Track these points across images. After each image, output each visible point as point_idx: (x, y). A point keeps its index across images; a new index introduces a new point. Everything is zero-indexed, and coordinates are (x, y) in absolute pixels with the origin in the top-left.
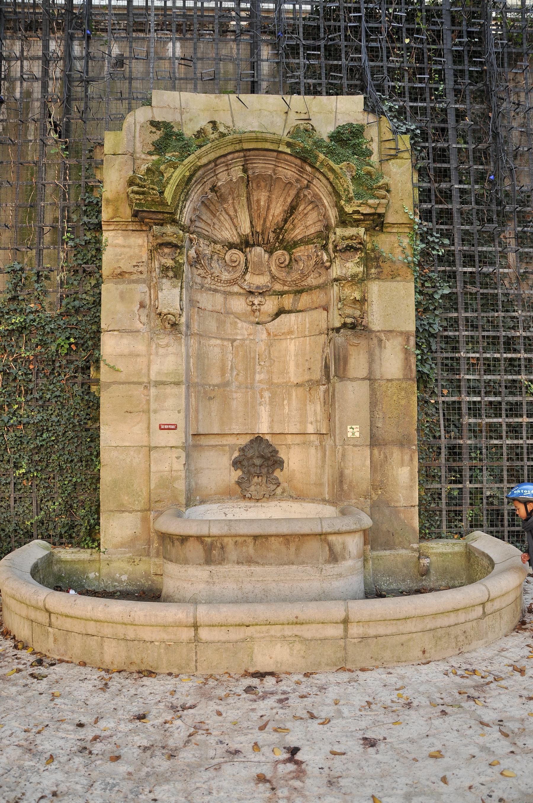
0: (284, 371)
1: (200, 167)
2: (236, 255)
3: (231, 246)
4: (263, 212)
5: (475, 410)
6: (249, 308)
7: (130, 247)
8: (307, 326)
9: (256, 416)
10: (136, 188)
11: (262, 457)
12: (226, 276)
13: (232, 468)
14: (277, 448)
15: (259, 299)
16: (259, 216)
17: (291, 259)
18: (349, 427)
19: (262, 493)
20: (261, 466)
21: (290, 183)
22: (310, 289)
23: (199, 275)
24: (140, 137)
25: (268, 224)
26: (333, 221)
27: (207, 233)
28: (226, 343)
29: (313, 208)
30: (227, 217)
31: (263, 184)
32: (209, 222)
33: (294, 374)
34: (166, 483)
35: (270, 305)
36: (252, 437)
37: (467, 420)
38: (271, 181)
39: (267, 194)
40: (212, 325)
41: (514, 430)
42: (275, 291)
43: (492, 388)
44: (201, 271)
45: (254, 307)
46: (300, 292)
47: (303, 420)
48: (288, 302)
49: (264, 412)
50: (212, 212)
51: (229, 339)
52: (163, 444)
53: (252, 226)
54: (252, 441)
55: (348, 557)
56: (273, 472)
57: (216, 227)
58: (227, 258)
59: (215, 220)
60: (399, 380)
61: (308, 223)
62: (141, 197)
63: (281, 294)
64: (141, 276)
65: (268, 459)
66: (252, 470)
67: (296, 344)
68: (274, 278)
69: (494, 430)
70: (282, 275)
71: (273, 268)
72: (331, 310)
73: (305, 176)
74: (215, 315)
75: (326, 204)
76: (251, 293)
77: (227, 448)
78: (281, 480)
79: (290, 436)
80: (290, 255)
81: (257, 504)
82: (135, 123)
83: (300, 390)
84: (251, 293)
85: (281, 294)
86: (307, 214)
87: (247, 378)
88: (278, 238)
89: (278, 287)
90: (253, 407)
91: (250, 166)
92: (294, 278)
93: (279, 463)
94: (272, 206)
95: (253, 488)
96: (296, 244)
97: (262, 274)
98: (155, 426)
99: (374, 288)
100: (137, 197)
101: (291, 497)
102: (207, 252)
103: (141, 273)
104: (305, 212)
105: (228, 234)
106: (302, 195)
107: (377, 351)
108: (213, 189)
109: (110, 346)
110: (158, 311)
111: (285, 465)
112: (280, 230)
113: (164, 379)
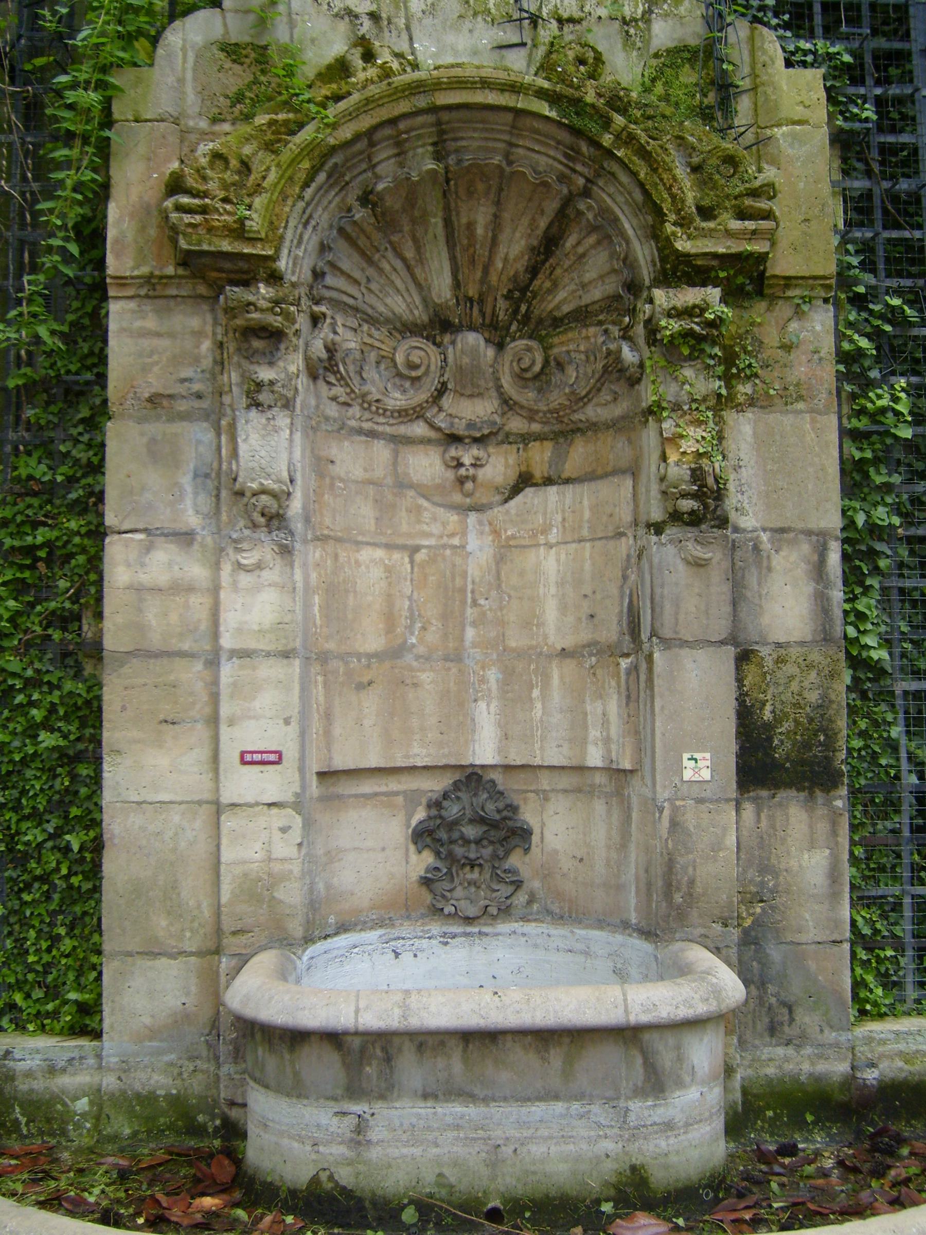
0: (531, 622)
1: (333, 149)
4: (482, 252)
6: (450, 475)
7: (171, 335)
8: (587, 514)
9: (467, 727)
10: (185, 200)
11: (482, 821)
12: (397, 399)
13: (412, 848)
14: (516, 800)
15: (475, 451)
16: (473, 262)
17: (546, 362)
18: (686, 756)
19: (483, 903)
20: (478, 842)
21: (545, 184)
22: (593, 428)
23: (334, 399)
24: (195, 79)
25: (493, 278)
26: (646, 274)
27: (351, 301)
28: (396, 556)
29: (599, 243)
30: (399, 264)
31: (480, 187)
32: (357, 274)
34: (259, 889)
36: (457, 776)
38: (500, 183)
39: (492, 210)
40: (365, 513)
42: (508, 435)
44: (339, 391)
45: (462, 471)
48: (540, 457)
50: (363, 254)
51: (403, 548)
52: (250, 799)
53: (457, 285)
54: (456, 785)
55: (687, 1079)
56: (507, 853)
57: (374, 286)
58: (400, 358)
59: (371, 271)
60: (802, 643)
61: (588, 276)
62: (198, 218)
63: (526, 439)
64: (197, 404)
65: (494, 825)
66: (459, 851)
68: (508, 404)
70: (528, 397)
71: (506, 382)
72: (643, 478)
73: (579, 168)
74: (371, 490)
75: (630, 232)
76: (454, 439)
77: (400, 799)
78: (525, 872)
79: (547, 772)
80: (546, 349)
81: (469, 929)
82: (184, 49)
83: (570, 665)
84: (454, 439)
85: (526, 439)
86: (583, 255)
87: (445, 635)
88: (516, 311)
89: (516, 424)
90: (461, 704)
91: (452, 145)
92: (554, 405)
94: (503, 237)
95: (459, 892)
96: (557, 322)
97: (480, 395)
98: (229, 754)
99: (743, 428)
100: (187, 218)
101: (549, 912)
102: (352, 345)
103: (199, 396)
104: (580, 250)
106: (570, 212)
107: (752, 579)
108: (365, 199)
109: (125, 566)
110: (237, 486)
111: (535, 839)
112: (521, 292)
113: (252, 645)
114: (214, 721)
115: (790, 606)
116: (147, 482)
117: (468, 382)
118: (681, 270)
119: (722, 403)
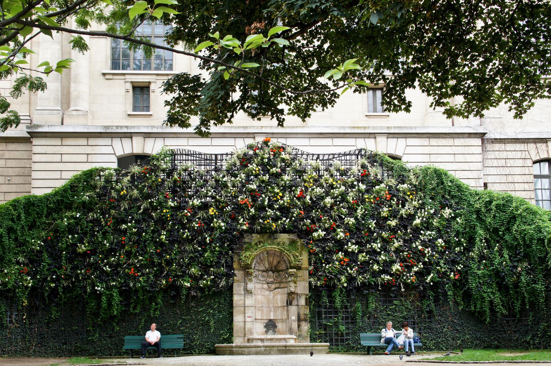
0: (277, 303)
2: (265, 274)
3: (263, 271)
9: (270, 314)
12: (262, 279)
22: (283, 282)
33: (279, 304)
40: (259, 291)
47: (282, 316)
48: (277, 285)
49: (272, 314)
67: (280, 297)
93: (276, 327)
98: (246, 316)
109: (236, 298)
112: (276, 267)
114: (245, 313)
116: (238, 289)
117: (269, 277)
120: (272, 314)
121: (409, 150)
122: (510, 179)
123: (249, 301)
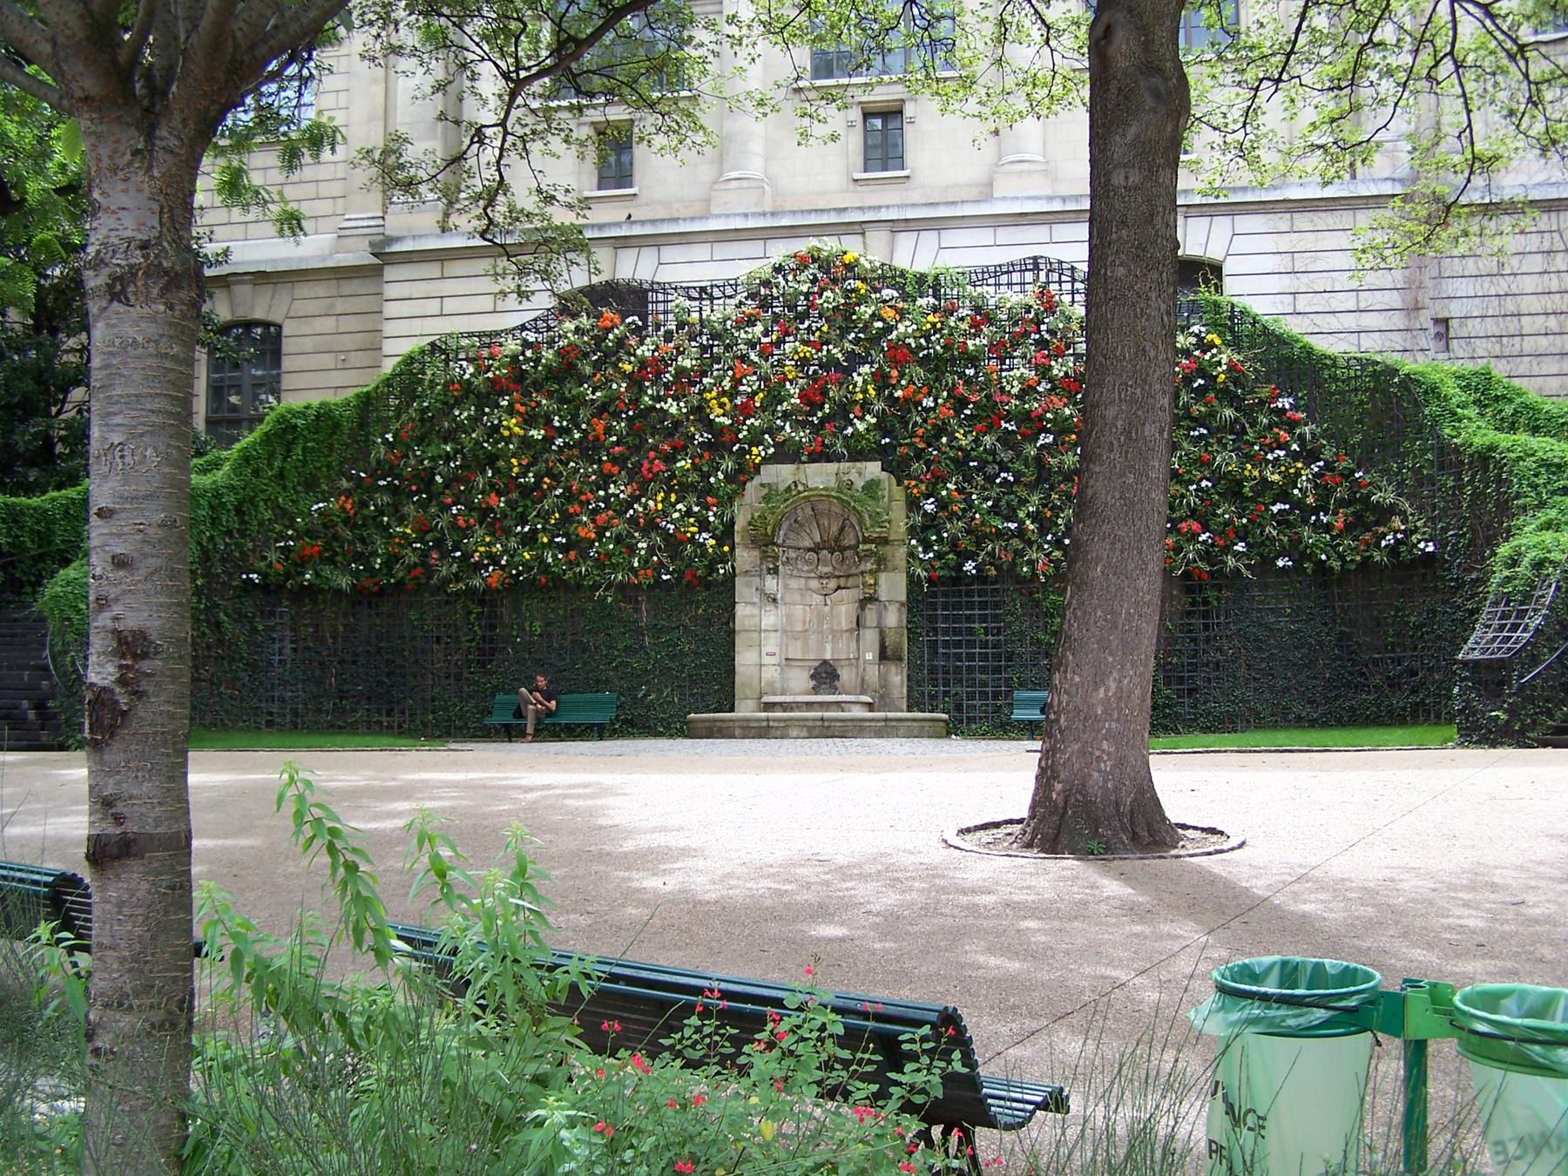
0: (839, 623)
3: (809, 550)
5: (946, 644)
34: (771, 684)
35: (833, 584)
37: (941, 650)
41: (971, 657)
43: (957, 632)
46: (848, 576)
48: (842, 582)
49: (828, 647)
69: (958, 657)
99: (883, 577)
105: (807, 543)
109: (741, 611)
112: (837, 540)
115: (894, 618)
118: (866, 541)
119: (878, 570)
120: (828, 647)
121: (1240, 244)
122: (1510, 305)
123: (770, 618)
